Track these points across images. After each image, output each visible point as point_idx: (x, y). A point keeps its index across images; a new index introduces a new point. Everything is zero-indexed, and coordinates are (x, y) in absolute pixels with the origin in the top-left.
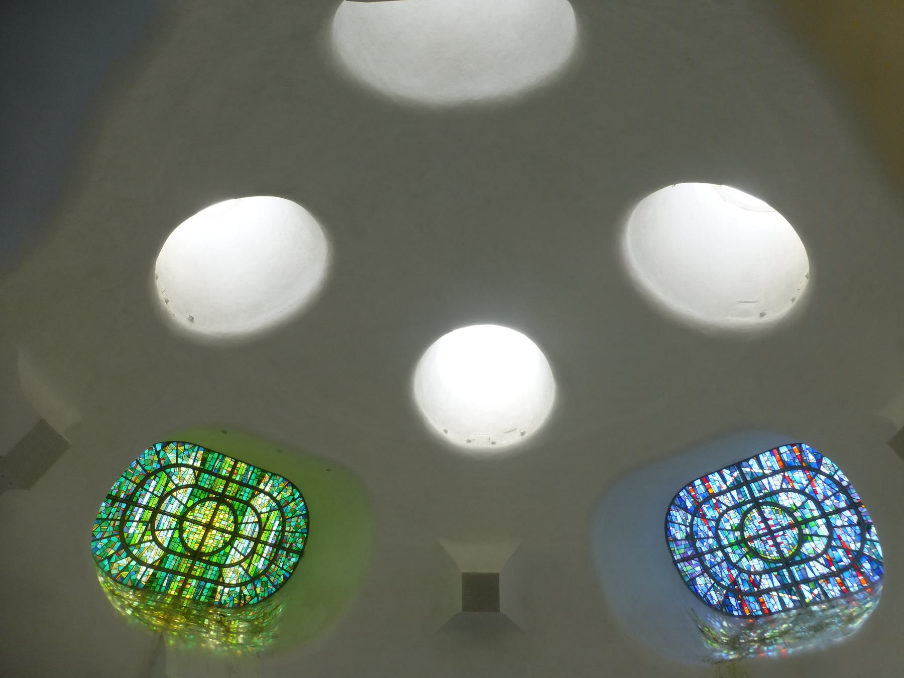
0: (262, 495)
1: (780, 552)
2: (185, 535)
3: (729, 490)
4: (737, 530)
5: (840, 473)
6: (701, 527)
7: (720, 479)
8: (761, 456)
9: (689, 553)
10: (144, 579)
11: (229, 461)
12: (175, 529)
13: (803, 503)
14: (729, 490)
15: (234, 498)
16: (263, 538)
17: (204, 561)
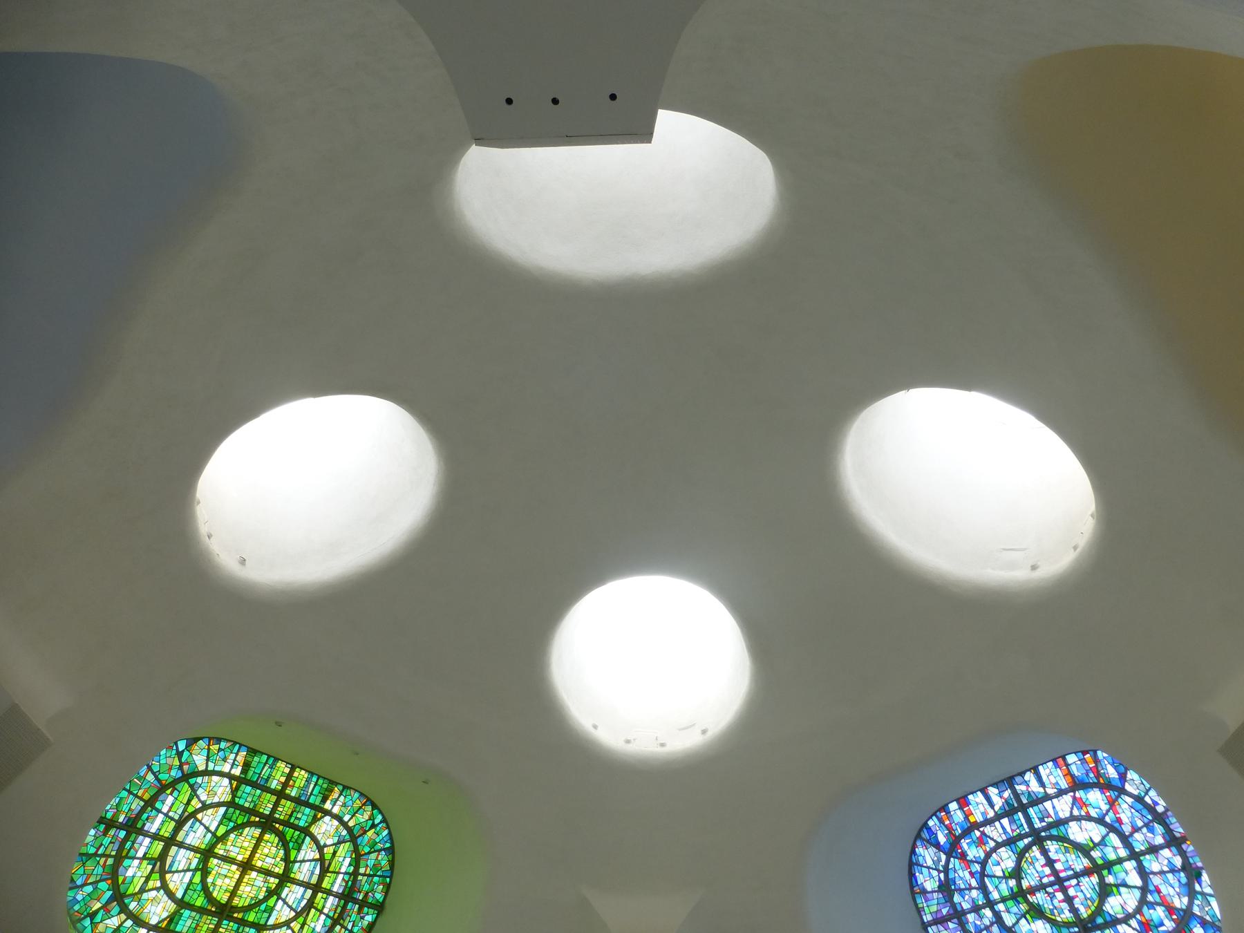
0: (327, 818)
1: (1074, 910)
2: (210, 880)
3: (998, 817)
4: (1011, 877)
5: (1152, 793)
6: (960, 872)
7: (985, 802)
8: (1040, 768)
9: (945, 911)
11: (283, 768)
12: (196, 870)
13: (1103, 838)
14: (998, 817)
15: (286, 824)
16: (325, 885)
17: (236, 920)
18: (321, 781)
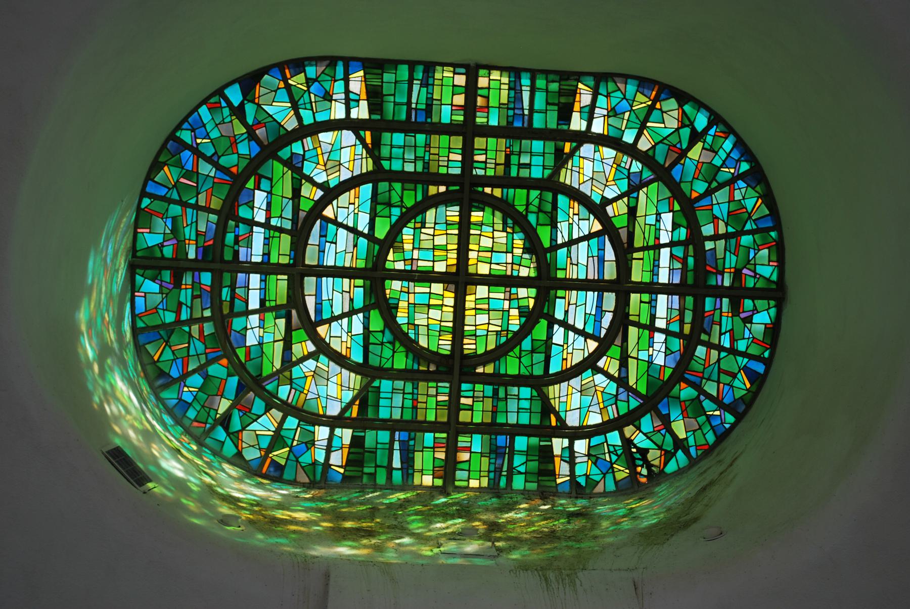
0: (587, 149)
2: (402, 318)
10: (336, 459)
11: (450, 79)
12: (365, 309)
16: (638, 274)
17: (485, 379)
18: (541, 83)
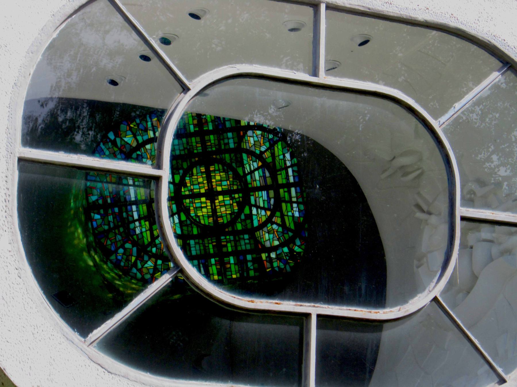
2: (192, 214)
